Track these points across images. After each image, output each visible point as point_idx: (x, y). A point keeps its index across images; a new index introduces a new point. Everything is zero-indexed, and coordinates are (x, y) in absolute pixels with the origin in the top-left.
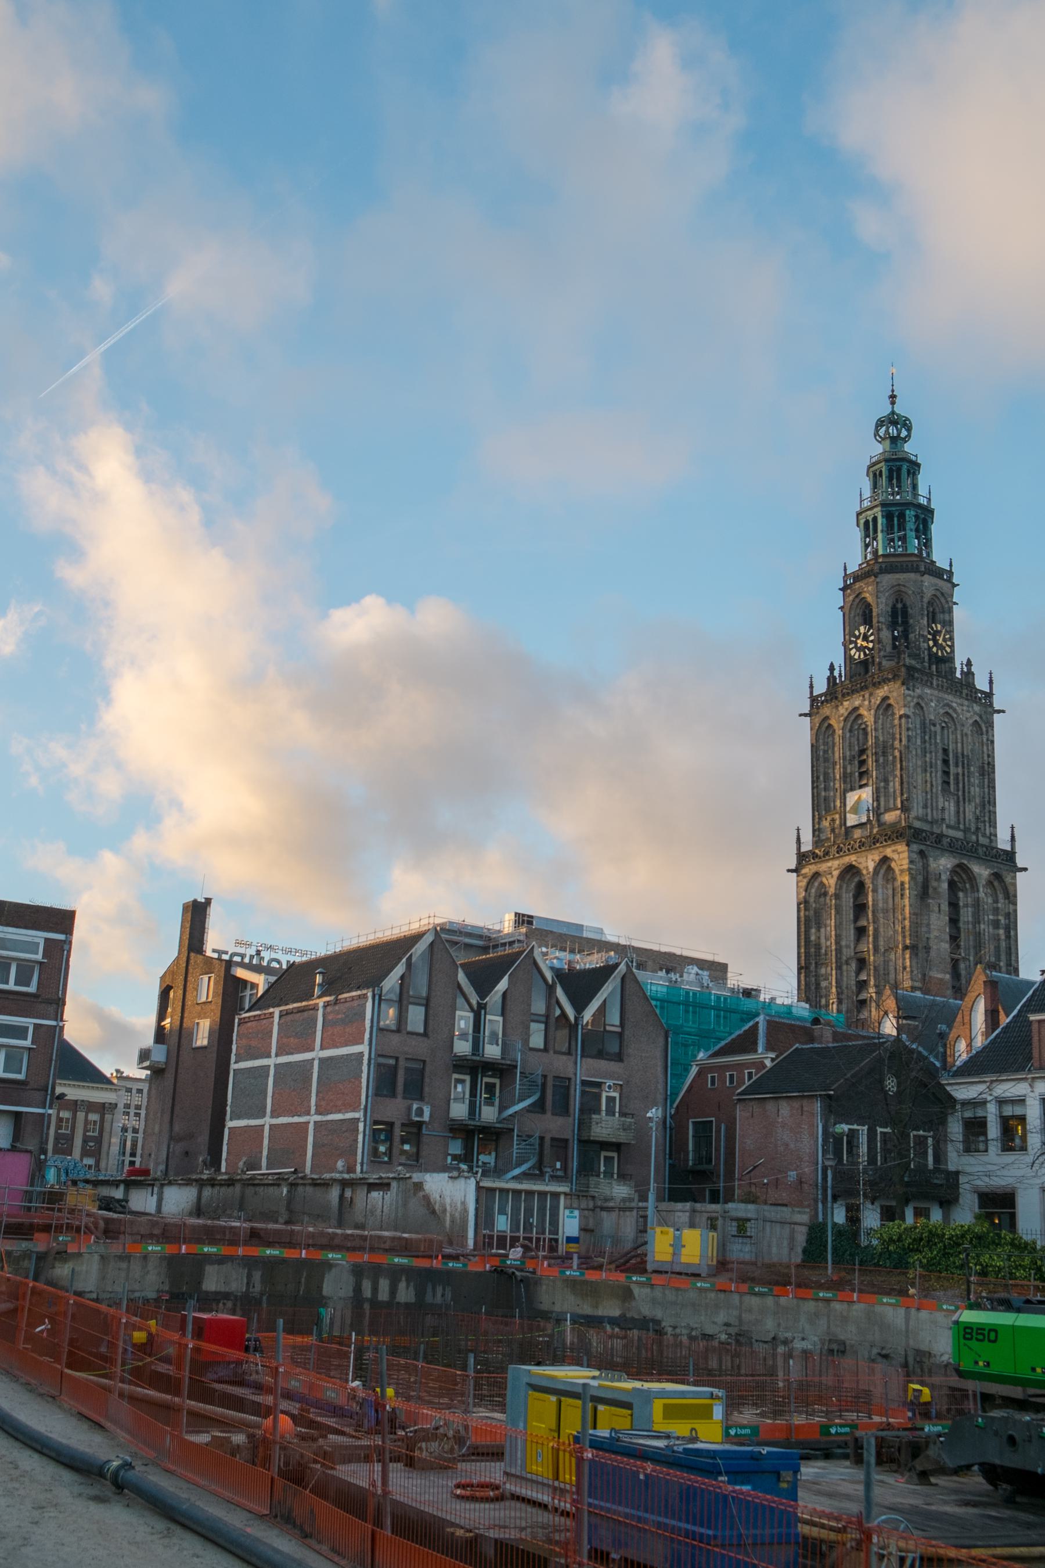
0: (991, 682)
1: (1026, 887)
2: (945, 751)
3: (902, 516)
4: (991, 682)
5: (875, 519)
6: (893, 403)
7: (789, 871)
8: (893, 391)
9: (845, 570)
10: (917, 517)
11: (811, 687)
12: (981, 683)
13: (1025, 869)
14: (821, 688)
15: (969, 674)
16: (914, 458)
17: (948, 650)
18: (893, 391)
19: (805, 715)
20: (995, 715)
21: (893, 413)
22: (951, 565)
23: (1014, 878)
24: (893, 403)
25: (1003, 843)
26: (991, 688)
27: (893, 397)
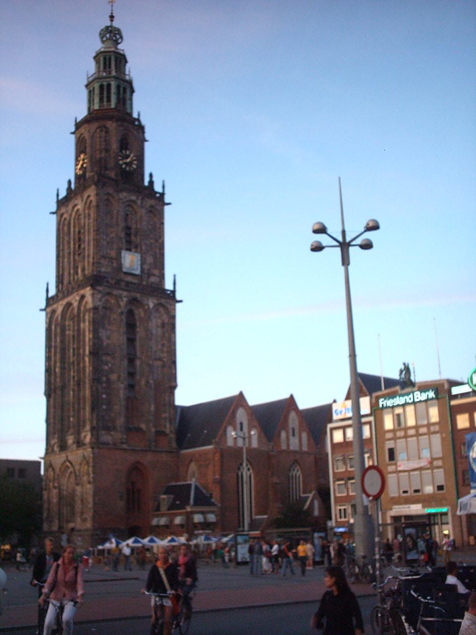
0: (163, 187)
1: (180, 311)
2: (128, 228)
3: (109, 86)
4: (163, 187)
5: (94, 88)
6: (112, 21)
7: (41, 310)
8: (112, 13)
9: (76, 121)
10: (118, 87)
11: (58, 195)
12: (158, 188)
13: (181, 301)
14: (63, 194)
15: (151, 183)
16: (122, 52)
18: (112, 13)
19: (53, 213)
21: (111, 26)
22: (139, 115)
23: (174, 306)
24: (112, 21)
25: (169, 286)
26: (164, 190)
27: (112, 17)
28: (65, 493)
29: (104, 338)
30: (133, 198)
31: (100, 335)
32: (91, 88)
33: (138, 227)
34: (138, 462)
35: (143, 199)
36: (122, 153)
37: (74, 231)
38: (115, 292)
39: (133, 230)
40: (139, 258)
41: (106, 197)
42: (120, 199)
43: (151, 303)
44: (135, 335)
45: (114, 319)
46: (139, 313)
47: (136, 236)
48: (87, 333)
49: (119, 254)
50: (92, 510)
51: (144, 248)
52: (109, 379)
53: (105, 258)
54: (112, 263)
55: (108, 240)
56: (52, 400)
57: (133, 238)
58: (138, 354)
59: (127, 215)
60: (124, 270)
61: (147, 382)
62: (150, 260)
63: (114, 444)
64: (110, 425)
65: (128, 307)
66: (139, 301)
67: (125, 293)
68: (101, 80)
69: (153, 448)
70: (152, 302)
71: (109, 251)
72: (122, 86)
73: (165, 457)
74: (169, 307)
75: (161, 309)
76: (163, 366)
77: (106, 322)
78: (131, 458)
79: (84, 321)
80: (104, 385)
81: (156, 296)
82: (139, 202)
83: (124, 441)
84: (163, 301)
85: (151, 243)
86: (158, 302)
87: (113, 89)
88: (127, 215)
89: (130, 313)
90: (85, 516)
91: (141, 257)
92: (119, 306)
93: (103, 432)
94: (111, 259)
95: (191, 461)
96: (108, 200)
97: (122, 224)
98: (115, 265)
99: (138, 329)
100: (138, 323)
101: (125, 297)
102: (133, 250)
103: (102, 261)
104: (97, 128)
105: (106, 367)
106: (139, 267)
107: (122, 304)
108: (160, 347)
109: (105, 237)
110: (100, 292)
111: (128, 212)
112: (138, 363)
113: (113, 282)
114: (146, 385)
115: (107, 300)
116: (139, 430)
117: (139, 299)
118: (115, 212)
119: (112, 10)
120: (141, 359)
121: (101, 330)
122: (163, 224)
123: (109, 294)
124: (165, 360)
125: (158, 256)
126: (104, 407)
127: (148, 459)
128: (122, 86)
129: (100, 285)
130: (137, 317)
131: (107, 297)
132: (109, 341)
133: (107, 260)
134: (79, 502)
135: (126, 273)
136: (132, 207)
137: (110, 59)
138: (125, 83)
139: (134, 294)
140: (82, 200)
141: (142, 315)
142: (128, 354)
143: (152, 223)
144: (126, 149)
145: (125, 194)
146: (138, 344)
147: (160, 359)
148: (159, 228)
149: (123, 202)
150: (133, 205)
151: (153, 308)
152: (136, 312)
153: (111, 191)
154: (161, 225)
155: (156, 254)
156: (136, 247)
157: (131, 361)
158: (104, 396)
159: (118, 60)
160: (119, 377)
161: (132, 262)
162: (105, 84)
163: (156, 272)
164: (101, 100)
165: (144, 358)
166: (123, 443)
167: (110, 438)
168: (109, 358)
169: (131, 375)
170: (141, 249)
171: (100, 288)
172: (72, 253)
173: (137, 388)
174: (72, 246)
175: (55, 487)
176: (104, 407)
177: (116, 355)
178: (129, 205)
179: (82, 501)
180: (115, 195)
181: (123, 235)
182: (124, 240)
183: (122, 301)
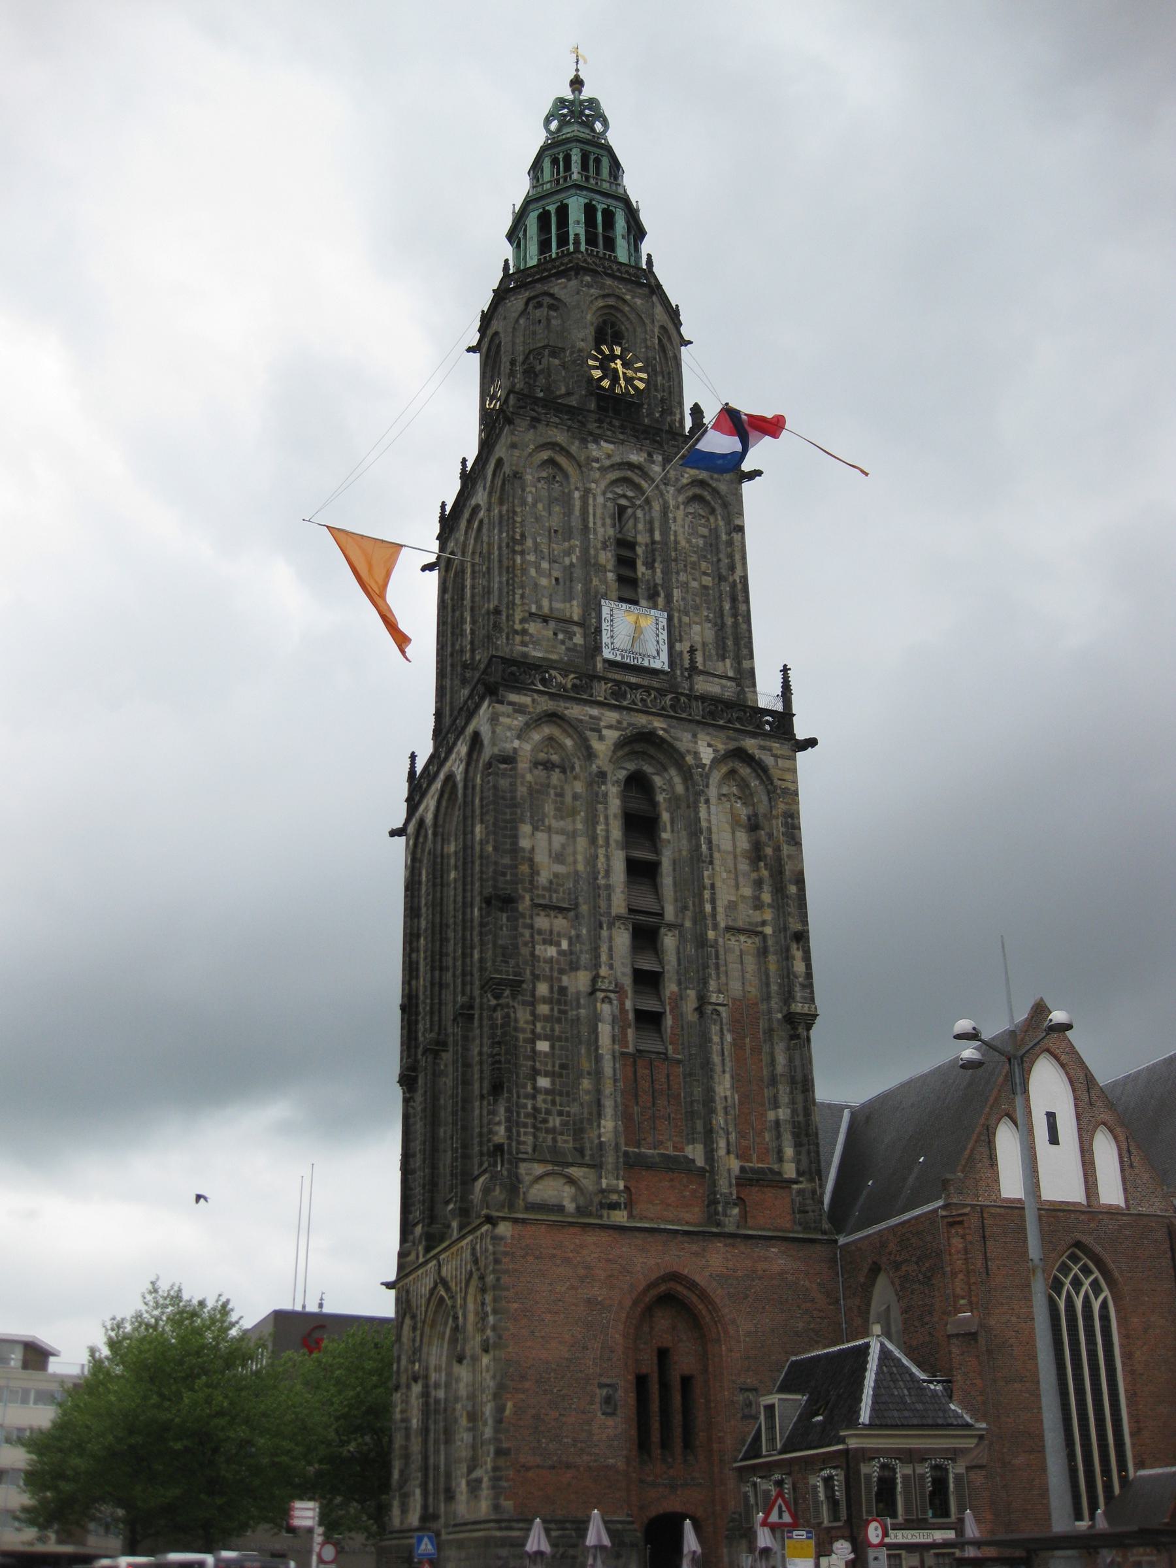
3: (563, 211)
10: (590, 210)
13: (812, 743)
17: (641, 386)
20: (747, 487)
29: (541, 858)
30: (635, 458)
31: (525, 843)
32: (521, 235)
33: (657, 537)
34: (675, 1277)
36: (601, 352)
38: (575, 711)
39: (640, 550)
40: (663, 622)
41: (545, 455)
42: (590, 459)
43: (705, 749)
44: (656, 851)
45: (575, 797)
46: (667, 784)
47: (650, 565)
49: (592, 606)
51: (677, 593)
52: (563, 990)
53: (545, 620)
54: (570, 636)
55: (555, 574)
56: (419, 1098)
57: (641, 569)
58: (670, 913)
59: (622, 510)
60: (607, 654)
61: (702, 1000)
62: (700, 632)
63: (580, 1211)
64: (566, 1143)
65: (631, 766)
66: (663, 740)
67: (612, 716)
68: (541, 203)
69: (730, 1228)
70: (709, 745)
71: (557, 605)
72: (600, 207)
73: (777, 1259)
74: (769, 760)
75: (745, 771)
76: (763, 952)
77: (549, 808)
78: (646, 1262)
80: (543, 1009)
81: (722, 727)
82: (657, 468)
83: (614, 1197)
84: (751, 744)
85: (706, 587)
86: (732, 745)
87: (576, 214)
88: (622, 510)
89: (637, 784)
90: (478, 1473)
91: (670, 619)
92: (590, 755)
93: (539, 1169)
94: (565, 622)
95: (875, 1270)
96: (551, 462)
97: (603, 530)
98: (578, 639)
99: (665, 836)
100: (665, 816)
101: (609, 727)
102: (643, 602)
103: (533, 627)
104: (527, 304)
105: (552, 951)
106: (665, 648)
107: (599, 747)
108: (747, 891)
109: (545, 565)
110: (520, 709)
111: (623, 502)
112: (669, 941)
113: (569, 681)
114: (700, 1010)
115: (551, 739)
116: (677, 1166)
117: (661, 733)
118: (577, 495)
119: (577, 70)
120: (682, 925)
121: (526, 829)
122: (740, 529)
123: (553, 717)
124: (768, 930)
125: (729, 621)
126: (543, 1082)
127: (709, 1266)
128: (600, 207)
129: (519, 690)
130: (661, 798)
131: (547, 730)
132: (560, 869)
133: (552, 624)
134: (464, 1422)
135: (612, 664)
136: (637, 487)
137: (567, 159)
138: (610, 201)
139: (642, 720)
140: (484, 489)
141: (680, 789)
142: (631, 911)
143: (705, 531)
144: (617, 338)
145: (608, 447)
146: (667, 880)
147: (751, 932)
148: (730, 543)
149: (603, 470)
150: (637, 479)
151: (715, 762)
152: (658, 781)
153: (560, 437)
154: (736, 537)
155: (722, 616)
156: (652, 597)
157: (646, 936)
158: (543, 1046)
159: (592, 157)
160: (595, 979)
161: (638, 632)
162: (552, 208)
163: (727, 667)
164: (544, 246)
165: (688, 924)
166: (614, 1206)
167: (568, 1191)
168: (560, 923)
169: (648, 981)
170: (669, 598)
171: (525, 700)
173: (669, 1021)
176: (543, 1082)
177: (584, 908)
178: (625, 480)
180: (574, 449)
181: (606, 558)
182: (611, 576)
183: (601, 738)
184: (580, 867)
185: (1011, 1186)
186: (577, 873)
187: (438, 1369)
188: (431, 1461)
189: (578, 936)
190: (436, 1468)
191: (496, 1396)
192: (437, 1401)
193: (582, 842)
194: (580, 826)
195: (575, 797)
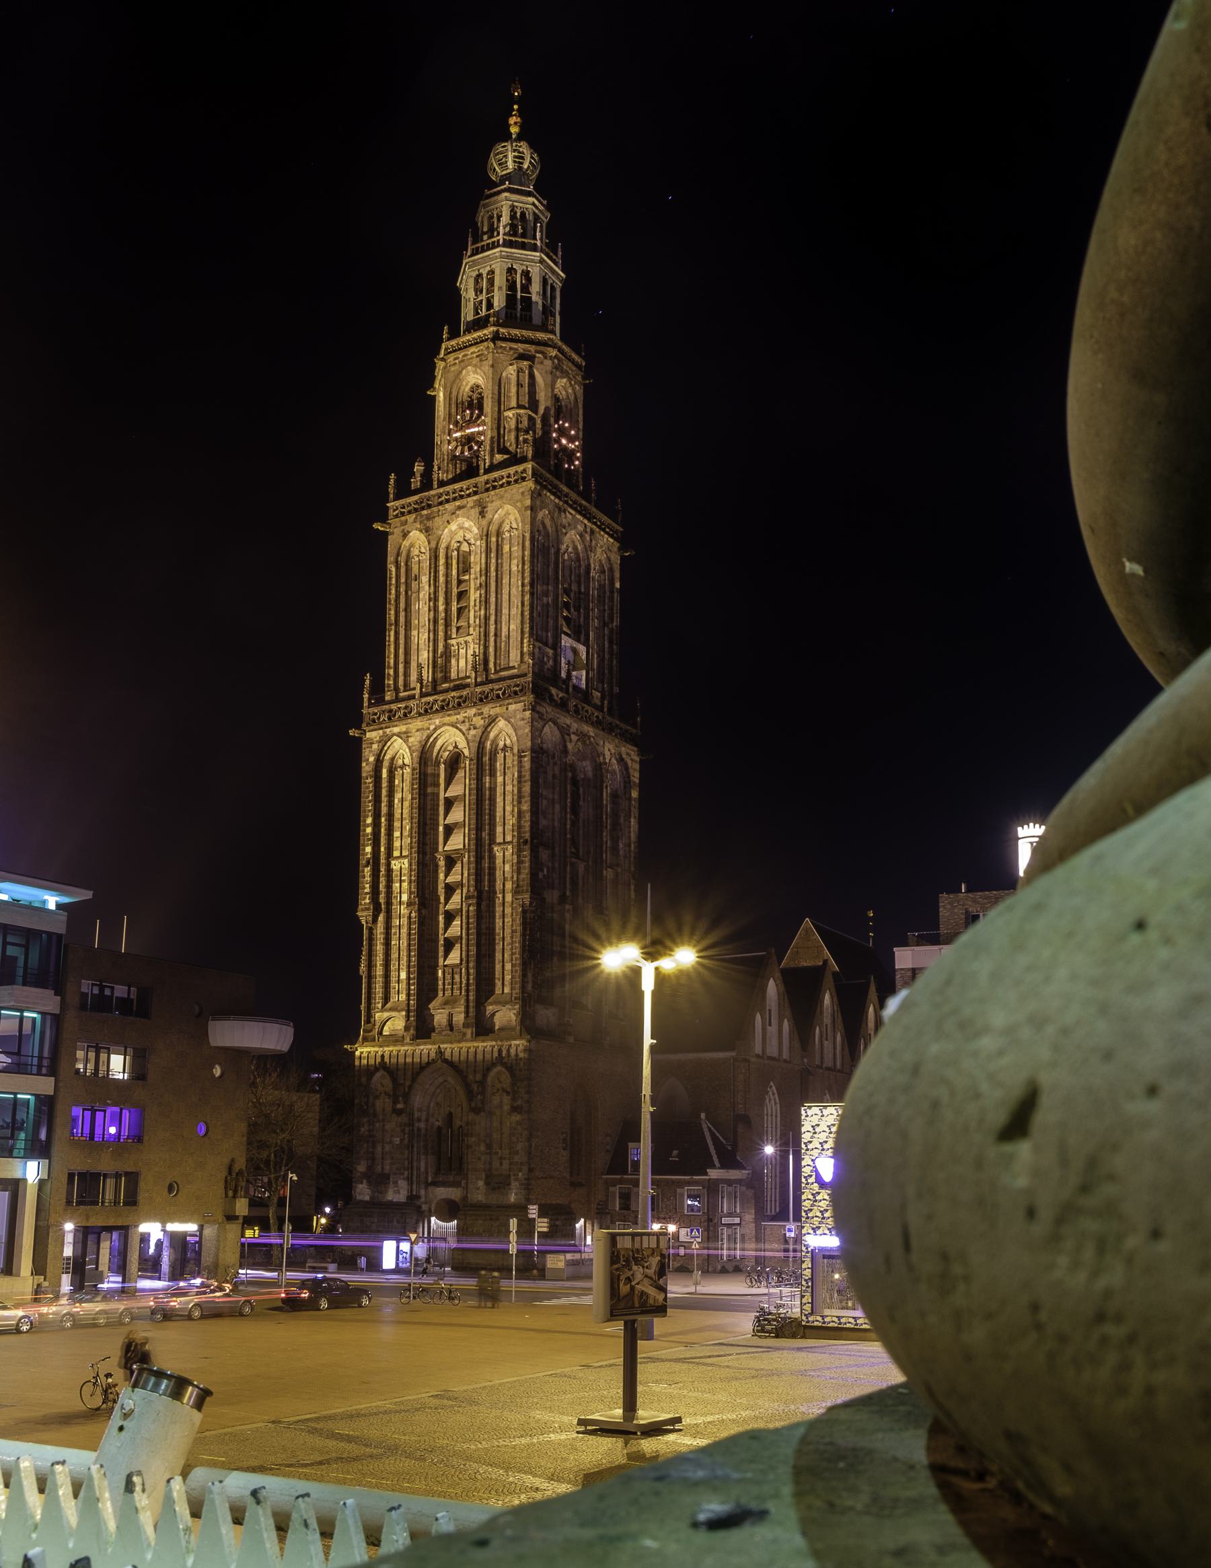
5: (492, 272)
28: (422, 1125)
32: (484, 272)
35: (592, 532)
37: (447, 575)
48: (499, 800)
50: (525, 1169)
72: (550, 282)
79: (493, 774)
118: (552, 551)
134: (483, 1148)
172: (441, 622)
174: (441, 608)
175: (399, 1113)
179: (489, 1146)
184: (556, 824)
185: (758, 1049)
186: (554, 827)
187: (420, 1110)
188: (415, 1164)
189: (553, 868)
190: (418, 1169)
191: (529, 1140)
192: (419, 1130)
193: (557, 807)
194: (556, 797)
195: (554, 776)
